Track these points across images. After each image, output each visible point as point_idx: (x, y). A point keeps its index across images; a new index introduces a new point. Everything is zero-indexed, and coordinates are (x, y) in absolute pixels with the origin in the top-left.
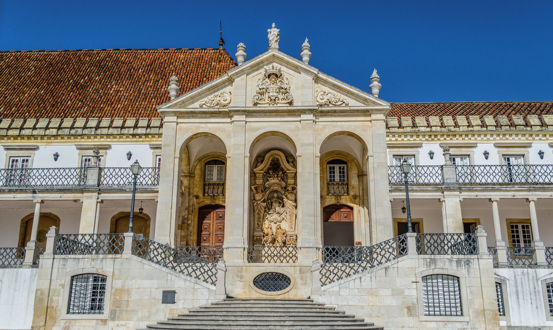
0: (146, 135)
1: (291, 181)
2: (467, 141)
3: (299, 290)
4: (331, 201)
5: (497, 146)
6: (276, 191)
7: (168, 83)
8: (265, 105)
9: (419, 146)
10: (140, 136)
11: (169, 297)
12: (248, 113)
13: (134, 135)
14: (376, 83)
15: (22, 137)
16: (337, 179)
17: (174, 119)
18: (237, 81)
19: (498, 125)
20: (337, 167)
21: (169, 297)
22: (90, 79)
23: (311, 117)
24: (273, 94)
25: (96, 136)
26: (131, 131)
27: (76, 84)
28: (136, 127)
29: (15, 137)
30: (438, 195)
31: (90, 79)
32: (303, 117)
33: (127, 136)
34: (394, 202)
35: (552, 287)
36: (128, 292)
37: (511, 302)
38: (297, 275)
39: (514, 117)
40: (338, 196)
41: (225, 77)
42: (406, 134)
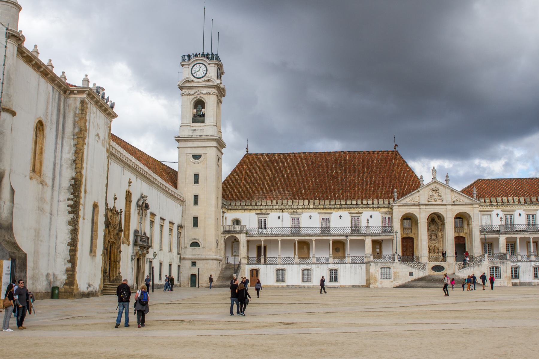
0: (378, 207)
1: (440, 227)
2: (512, 209)
3: (448, 271)
4: (457, 235)
5: (525, 210)
6: (433, 231)
7: (393, 193)
8: (433, 202)
9: (492, 211)
10: (376, 208)
11: (411, 274)
12: (426, 205)
13: (373, 208)
14: (475, 192)
15: (326, 208)
16: (459, 226)
17: (397, 207)
18: (421, 191)
19: (525, 202)
20: (458, 220)
21: (411, 274)
22: (337, 172)
23: (450, 206)
24: (436, 198)
25: (356, 208)
26: (371, 206)
27: (331, 174)
28: (373, 204)
29: (323, 209)
30: (497, 236)
31: (337, 172)
32: (448, 206)
33: (370, 208)
34: (481, 239)
35: (535, 268)
36: (398, 272)
37: (521, 274)
38: (447, 266)
39: (532, 198)
40: (459, 233)
41: (417, 191)
42: (487, 206)
